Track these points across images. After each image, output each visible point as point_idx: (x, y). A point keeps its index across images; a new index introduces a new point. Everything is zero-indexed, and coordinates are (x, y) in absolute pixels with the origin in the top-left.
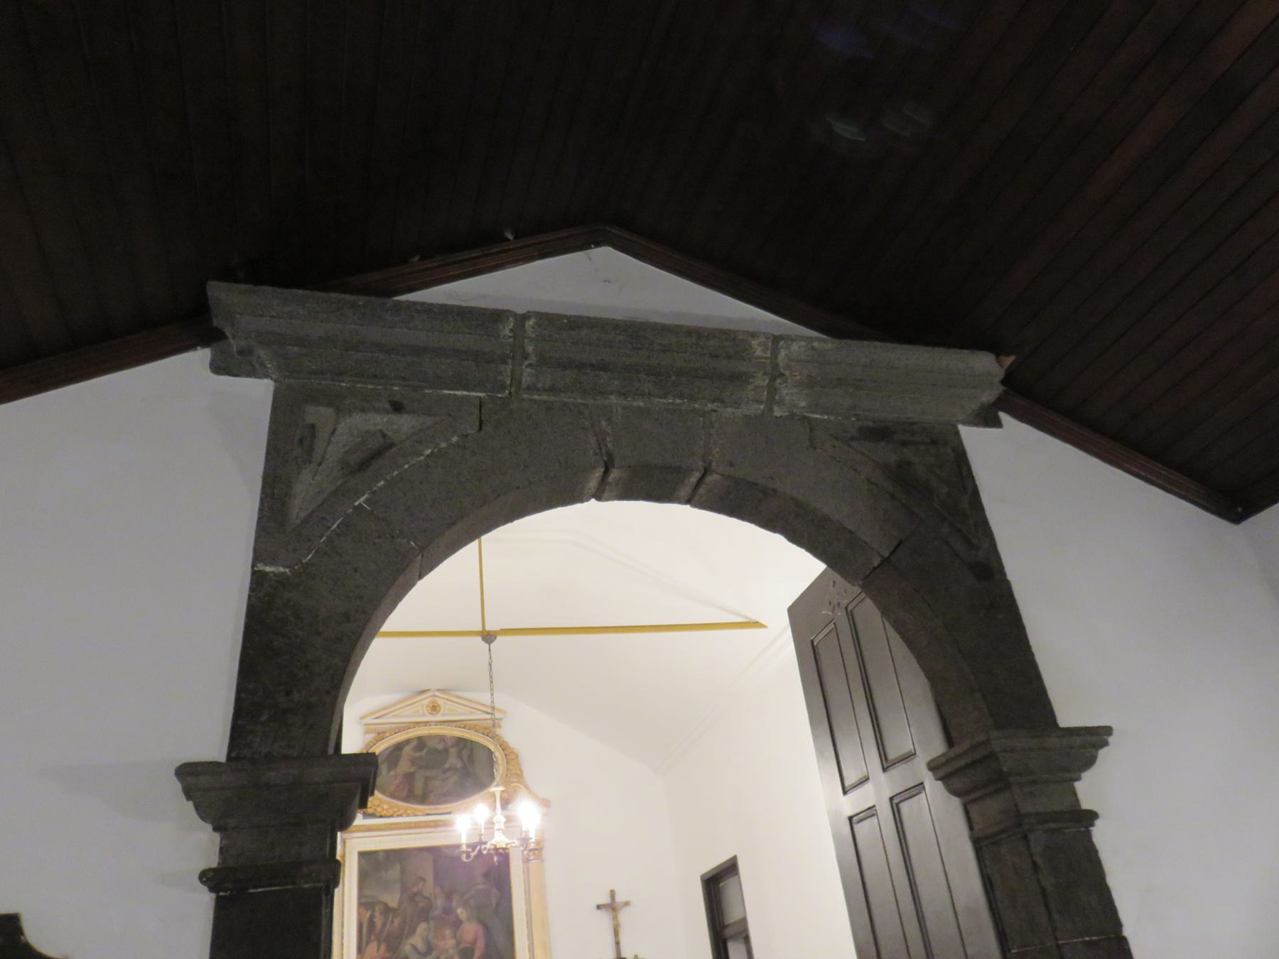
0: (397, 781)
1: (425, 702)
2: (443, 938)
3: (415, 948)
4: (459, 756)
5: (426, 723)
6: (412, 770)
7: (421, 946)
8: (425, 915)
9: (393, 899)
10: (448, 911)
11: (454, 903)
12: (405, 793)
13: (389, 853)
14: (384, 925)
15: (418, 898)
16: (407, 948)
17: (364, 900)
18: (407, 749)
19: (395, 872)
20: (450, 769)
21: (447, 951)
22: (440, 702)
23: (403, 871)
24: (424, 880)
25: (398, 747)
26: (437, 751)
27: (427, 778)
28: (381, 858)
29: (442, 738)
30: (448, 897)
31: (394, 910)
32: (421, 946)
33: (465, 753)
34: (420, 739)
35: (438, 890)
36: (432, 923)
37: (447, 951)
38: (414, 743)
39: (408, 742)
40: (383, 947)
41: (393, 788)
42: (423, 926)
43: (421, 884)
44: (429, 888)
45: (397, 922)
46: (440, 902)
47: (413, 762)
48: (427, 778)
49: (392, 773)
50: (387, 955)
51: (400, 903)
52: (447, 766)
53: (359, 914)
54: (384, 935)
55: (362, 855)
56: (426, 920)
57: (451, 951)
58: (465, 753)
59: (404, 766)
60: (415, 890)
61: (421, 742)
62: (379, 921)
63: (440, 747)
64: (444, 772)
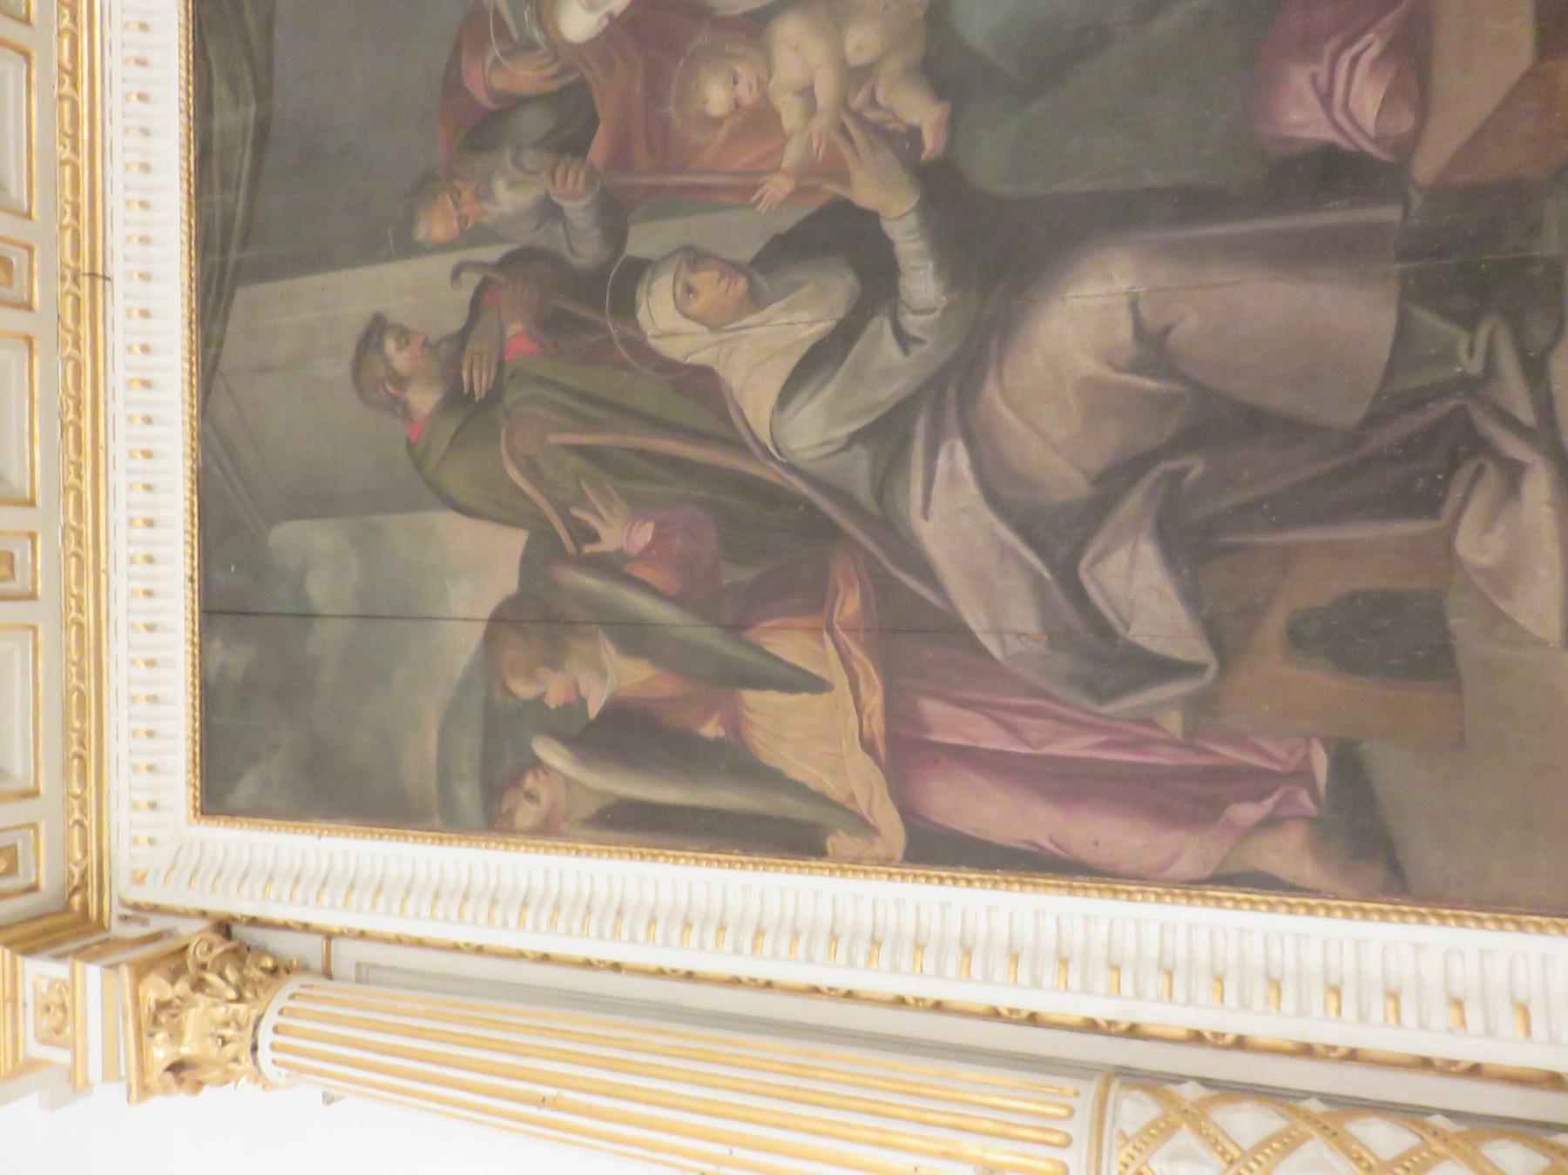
2: (759, 119)
3: (815, 363)
7: (799, 319)
8: (581, 299)
9: (480, 564)
10: (570, 121)
11: (526, 76)
13: (218, 610)
14: (634, 636)
15: (479, 380)
16: (811, 432)
17: (468, 795)
19: (317, 557)
21: (855, 76)
23: (314, 501)
24: (376, 329)
28: (236, 659)
30: (481, 130)
31: (544, 555)
32: (799, 319)
35: (435, 225)
36: (642, 241)
37: (855, 76)
40: (790, 644)
42: (663, 316)
43: (400, 358)
44: (417, 290)
45: (621, 532)
46: (509, 198)
50: (849, 604)
51: (500, 508)
53: (547, 830)
54: (706, 635)
55: (217, 794)
56: (620, 283)
57: (862, 41)
60: (424, 399)
62: (606, 676)
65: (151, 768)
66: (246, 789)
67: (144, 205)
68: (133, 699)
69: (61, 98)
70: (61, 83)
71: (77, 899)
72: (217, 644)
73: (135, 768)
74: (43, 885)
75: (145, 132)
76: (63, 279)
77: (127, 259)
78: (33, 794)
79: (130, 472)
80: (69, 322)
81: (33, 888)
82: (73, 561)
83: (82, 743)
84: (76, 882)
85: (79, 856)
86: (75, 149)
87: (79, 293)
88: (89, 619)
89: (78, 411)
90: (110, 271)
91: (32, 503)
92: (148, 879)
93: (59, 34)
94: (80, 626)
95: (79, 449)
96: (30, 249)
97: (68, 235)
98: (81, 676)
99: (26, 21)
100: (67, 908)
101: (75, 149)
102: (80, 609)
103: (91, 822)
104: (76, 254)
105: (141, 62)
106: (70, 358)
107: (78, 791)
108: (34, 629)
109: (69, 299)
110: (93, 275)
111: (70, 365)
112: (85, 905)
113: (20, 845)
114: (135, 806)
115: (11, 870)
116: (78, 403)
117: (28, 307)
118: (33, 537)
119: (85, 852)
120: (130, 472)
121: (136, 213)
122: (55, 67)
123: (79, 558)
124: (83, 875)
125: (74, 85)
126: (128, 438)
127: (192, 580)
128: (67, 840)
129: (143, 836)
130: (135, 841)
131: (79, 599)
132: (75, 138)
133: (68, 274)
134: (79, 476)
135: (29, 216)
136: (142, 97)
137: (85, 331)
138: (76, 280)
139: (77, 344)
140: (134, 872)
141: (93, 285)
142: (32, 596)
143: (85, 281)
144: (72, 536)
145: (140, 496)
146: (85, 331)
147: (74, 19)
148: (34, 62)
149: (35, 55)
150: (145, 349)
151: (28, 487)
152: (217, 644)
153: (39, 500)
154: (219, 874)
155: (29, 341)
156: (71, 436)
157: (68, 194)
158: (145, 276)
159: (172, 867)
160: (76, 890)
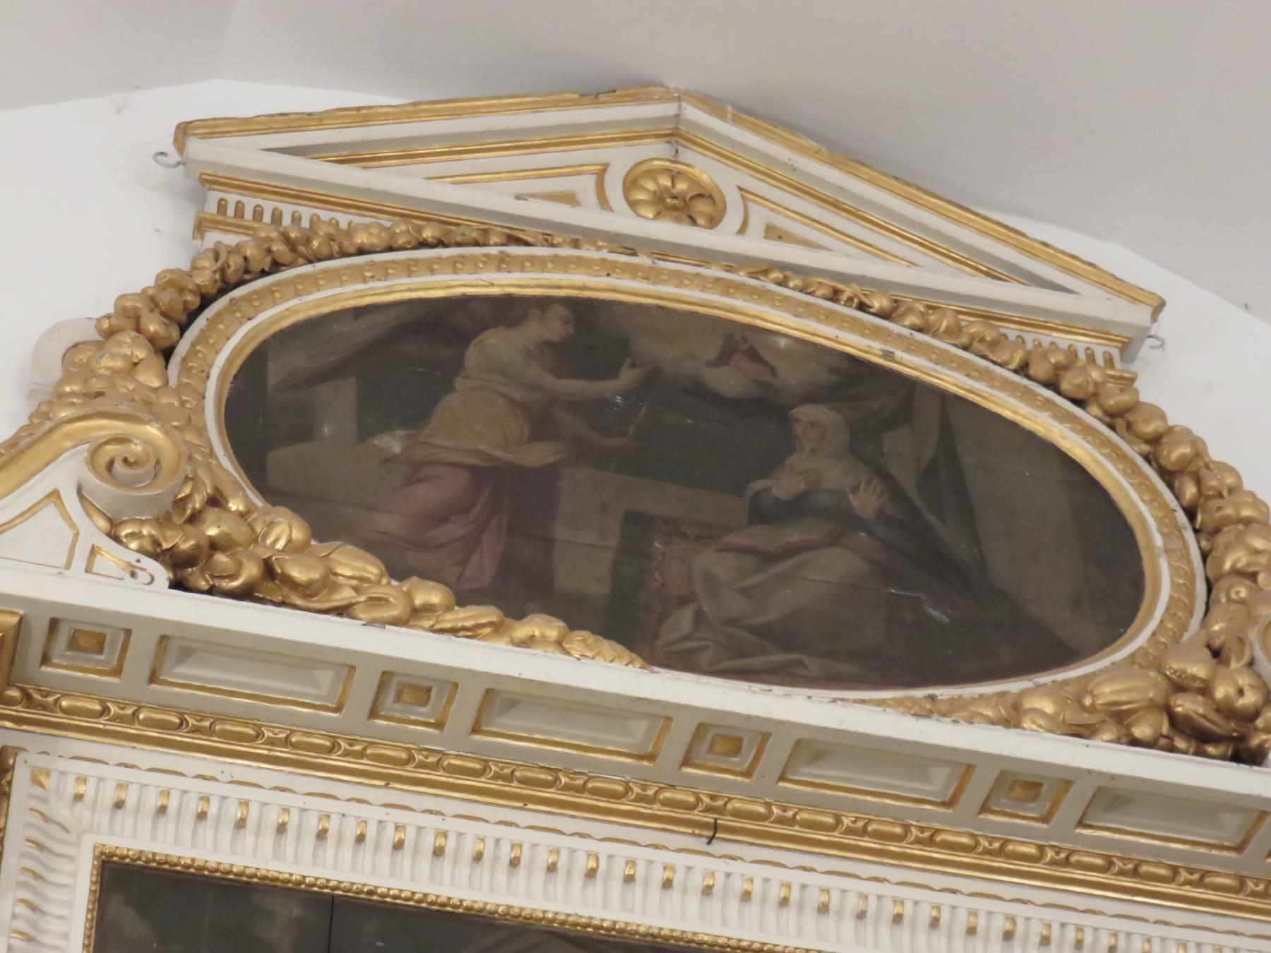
0: (428, 495)
1: (622, 158)
4: (863, 443)
5: (630, 246)
6: (539, 455)
12: (483, 565)
18: (498, 344)
20: (796, 508)
22: (706, 169)
25: (443, 329)
26: (700, 391)
27: (637, 523)
29: (741, 342)
33: (905, 451)
34: (584, 311)
38: (554, 327)
39: (506, 310)
41: (390, 523)
47: (541, 422)
48: (637, 523)
49: (392, 443)
52: (783, 486)
58: (905, 451)
59: (473, 423)
61: (591, 333)
63: (729, 381)
64: (762, 514)
65: (162, 810)
66: (131, 922)
67: (784, 902)
68: (245, 803)
69: (907, 828)
70: (922, 829)
71: (14, 693)
72: (296, 911)
73: (166, 793)
74: (43, 668)
75: (861, 915)
76: (713, 798)
77: (728, 875)
78: (153, 678)
79: (498, 841)
80: (668, 794)
81: (45, 660)
82: (404, 755)
83: (196, 730)
84: (37, 697)
85: (64, 703)
86: (850, 831)
87: (696, 812)
88: (335, 760)
89: (568, 788)
90: (718, 848)
91: (475, 730)
92: (37, 790)
93: (973, 836)
94: (331, 750)
95: (526, 782)
96: (748, 774)
97: (762, 810)
98: (272, 742)
99: (984, 809)
100: (10, 684)
101: (850, 831)
102: (347, 753)
103: (100, 724)
104: (738, 814)
105: (935, 923)
106: (628, 789)
107: (141, 716)
108: (338, 709)
109: (691, 799)
110: (716, 827)
111: (620, 788)
112: (10, 702)
113: (101, 657)
114: (121, 786)
115: (73, 644)
116: (582, 789)
117: (686, 762)
118: (439, 725)
119: (68, 712)
120: (498, 841)
121: (776, 892)
122: (938, 826)
123: (407, 762)
124: (44, 707)
125: (918, 841)
126: (535, 846)
127: (371, 893)
128: (88, 696)
129: (88, 790)
130: (82, 780)
131: (361, 754)
132: (863, 832)
133: (720, 803)
134: (496, 777)
135: (782, 778)
136: (898, 919)
137: (656, 809)
138: (709, 809)
139: (640, 799)
140: (48, 773)
141: (704, 826)
142: (373, 714)
143: (709, 818)
144: (432, 759)
145: (470, 847)
146: (656, 809)
147: (988, 852)
148: (942, 810)
149: (950, 811)
150: (629, 879)
151: (494, 729)
152: (296, 911)
153: (477, 737)
154: (37, 876)
155: (651, 757)
156: (543, 776)
157: (805, 816)
158: (707, 891)
159: (46, 818)
160: (27, 696)
